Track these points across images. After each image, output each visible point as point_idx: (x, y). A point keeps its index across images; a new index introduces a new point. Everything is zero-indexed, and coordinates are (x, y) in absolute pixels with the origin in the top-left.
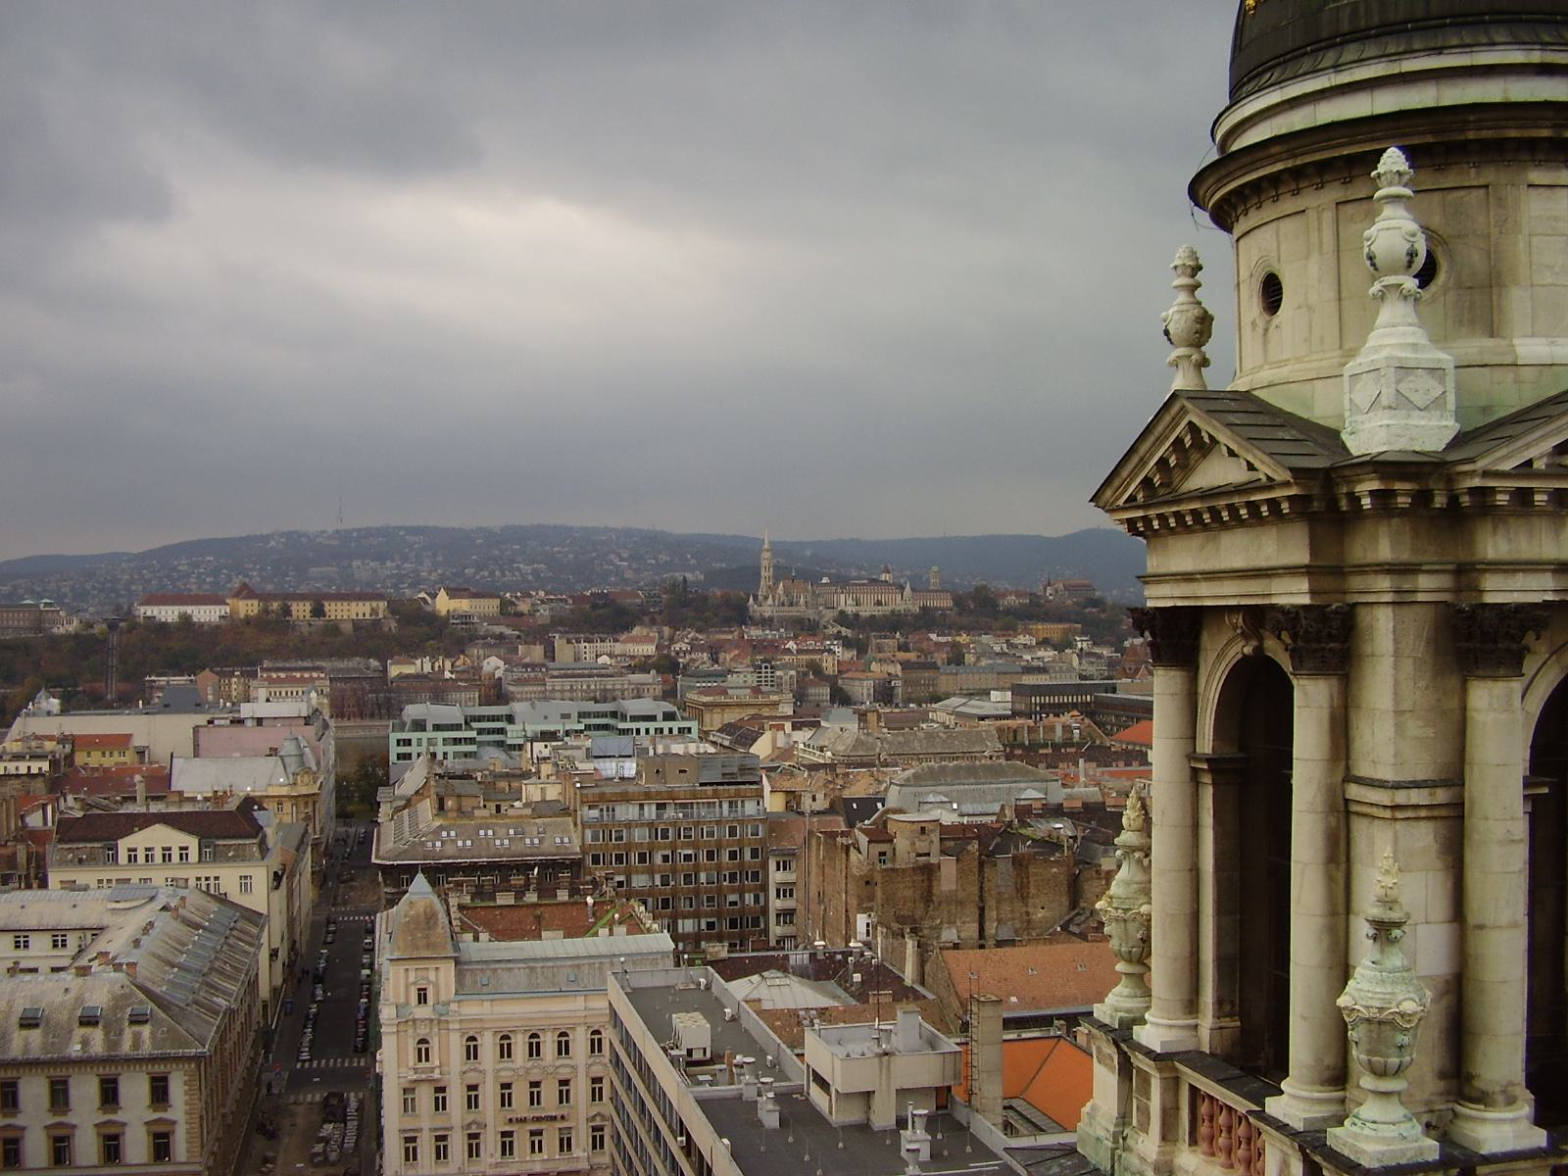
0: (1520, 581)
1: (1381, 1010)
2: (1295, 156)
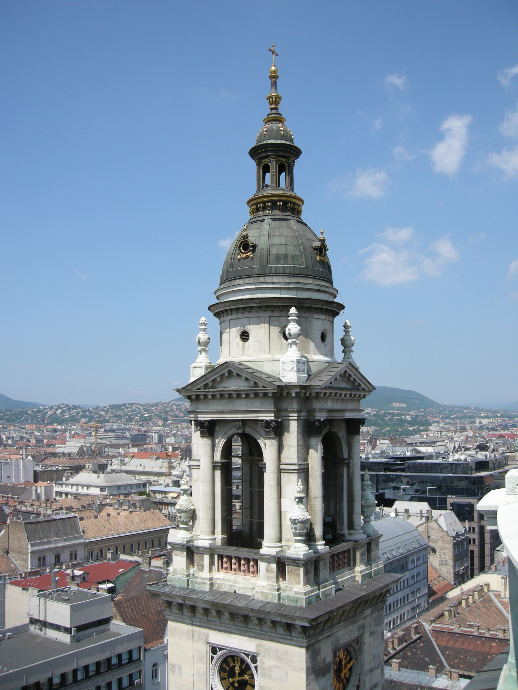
1: (303, 518)
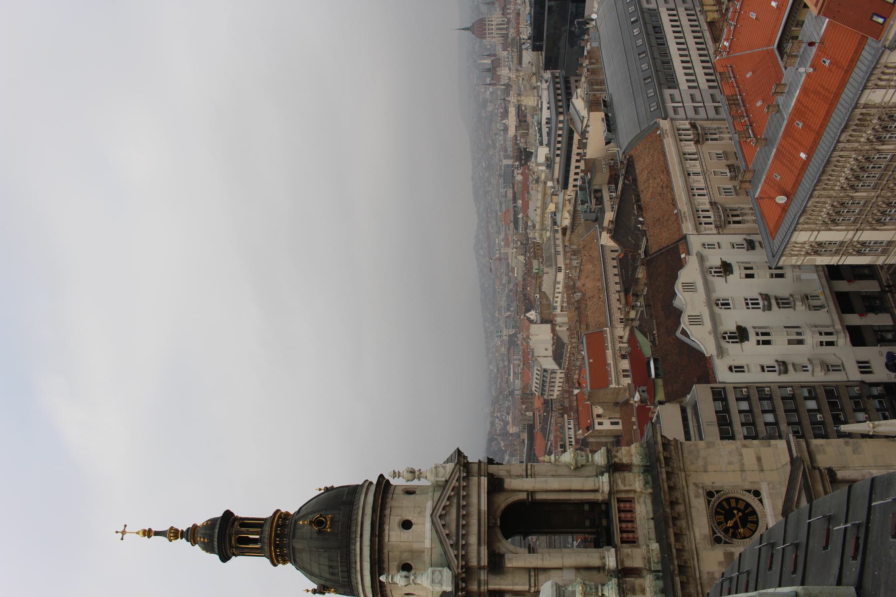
0: (482, 556)
1: (581, 594)
2: (378, 593)
